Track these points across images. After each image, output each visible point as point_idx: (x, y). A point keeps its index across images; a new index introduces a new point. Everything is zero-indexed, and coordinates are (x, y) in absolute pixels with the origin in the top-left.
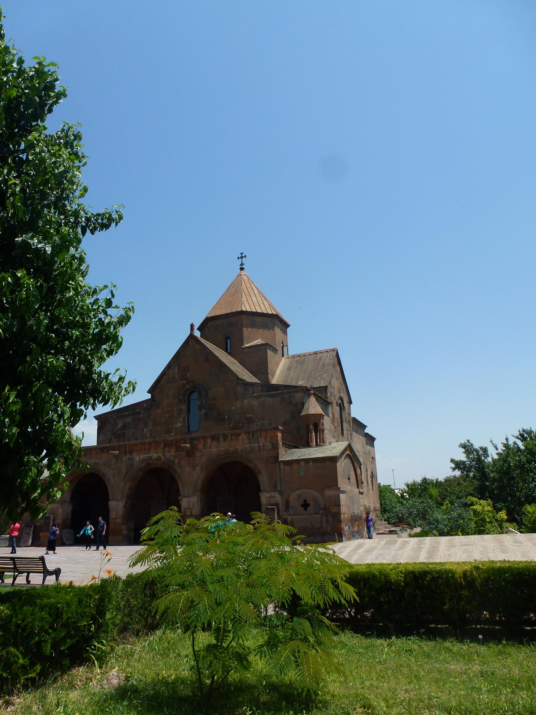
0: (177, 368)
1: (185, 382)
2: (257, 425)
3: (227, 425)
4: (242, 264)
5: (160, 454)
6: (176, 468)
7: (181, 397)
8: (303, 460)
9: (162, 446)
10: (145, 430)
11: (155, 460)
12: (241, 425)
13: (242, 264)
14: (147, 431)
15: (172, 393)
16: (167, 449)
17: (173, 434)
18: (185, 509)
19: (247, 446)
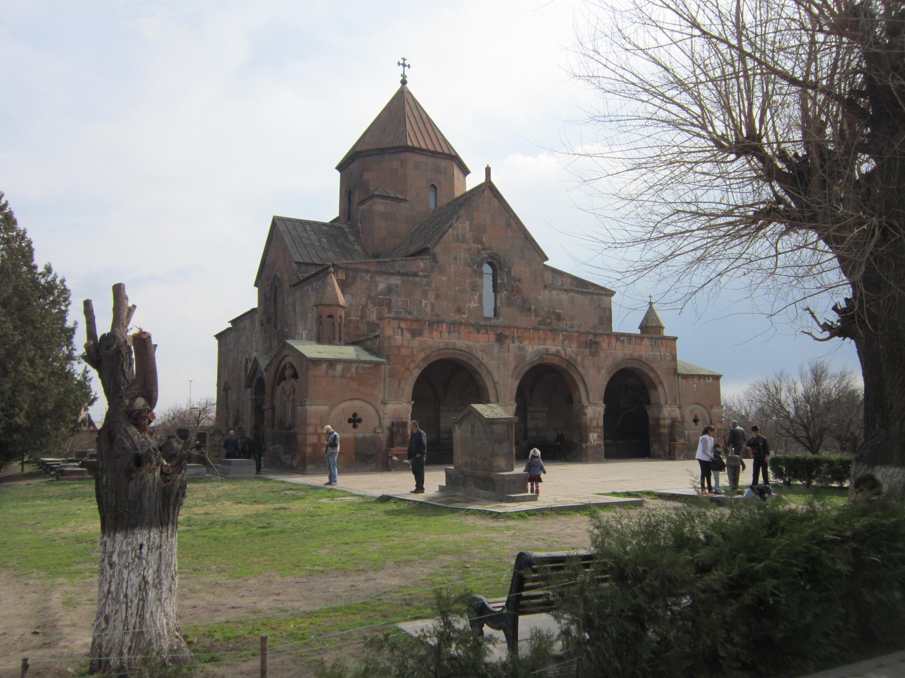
0: (467, 222)
1: (480, 246)
2: (566, 324)
3: (533, 318)
4: (404, 76)
5: (559, 348)
6: (580, 369)
7: (475, 267)
9: (561, 337)
10: (424, 302)
12: (549, 321)
13: (404, 76)
14: (426, 304)
16: (567, 342)
17: (465, 316)
18: (591, 419)
19: (650, 353)
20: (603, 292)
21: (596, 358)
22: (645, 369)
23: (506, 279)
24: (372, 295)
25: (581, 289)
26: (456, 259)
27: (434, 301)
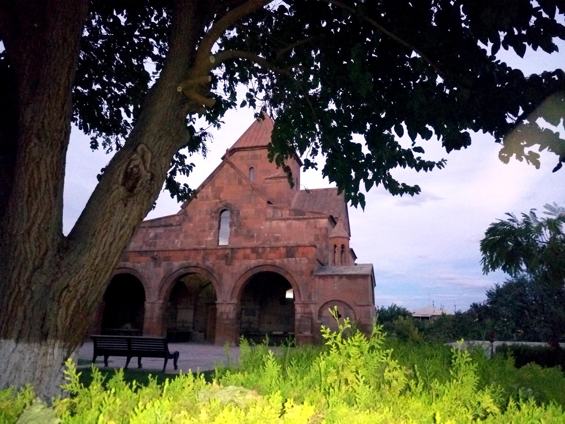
0: (210, 187)
1: (218, 200)
3: (255, 242)
6: (215, 275)
7: (213, 214)
8: (337, 275)
10: (176, 241)
11: (195, 267)
14: (178, 242)
15: (205, 209)
18: (222, 313)
20: (318, 216)
21: (231, 266)
22: (282, 273)
23: (235, 219)
24: (146, 240)
25: (296, 217)
26: (200, 211)
27: (182, 240)
